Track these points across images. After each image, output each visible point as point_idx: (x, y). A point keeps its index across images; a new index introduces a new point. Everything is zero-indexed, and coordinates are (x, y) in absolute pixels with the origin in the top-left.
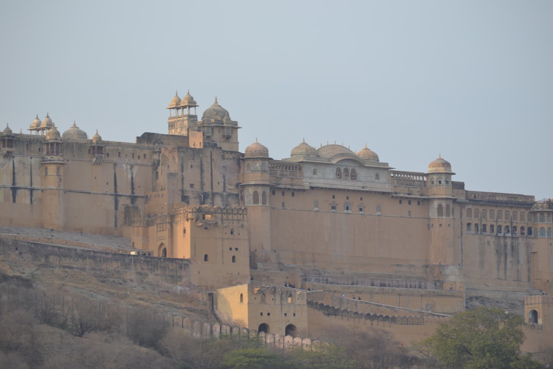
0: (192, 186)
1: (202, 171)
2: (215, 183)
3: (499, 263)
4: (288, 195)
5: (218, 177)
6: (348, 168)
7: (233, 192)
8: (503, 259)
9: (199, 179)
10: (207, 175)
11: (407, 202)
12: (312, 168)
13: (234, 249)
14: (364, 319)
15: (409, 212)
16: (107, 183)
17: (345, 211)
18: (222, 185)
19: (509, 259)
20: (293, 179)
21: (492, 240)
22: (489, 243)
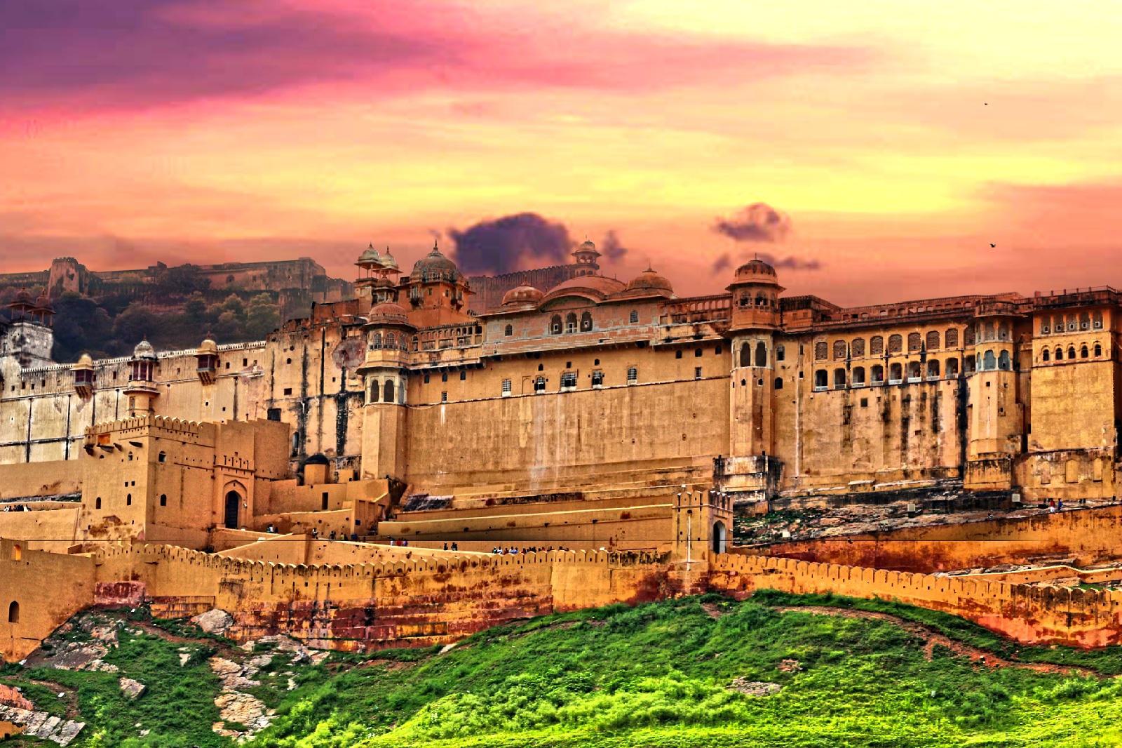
0: (288, 392)
1: (305, 366)
2: (327, 381)
3: (887, 437)
4: (454, 380)
5: (333, 371)
6: (576, 312)
7: (357, 390)
8: (897, 429)
9: (300, 379)
10: (314, 371)
11: (692, 354)
12: (504, 323)
13: (130, 484)
14: (291, 574)
15: (698, 370)
16: (224, 409)
17: (564, 389)
18: (339, 381)
19: (913, 426)
20: (463, 351)
21: (873, 396)
22: (864, 403)
